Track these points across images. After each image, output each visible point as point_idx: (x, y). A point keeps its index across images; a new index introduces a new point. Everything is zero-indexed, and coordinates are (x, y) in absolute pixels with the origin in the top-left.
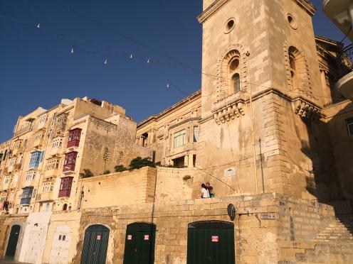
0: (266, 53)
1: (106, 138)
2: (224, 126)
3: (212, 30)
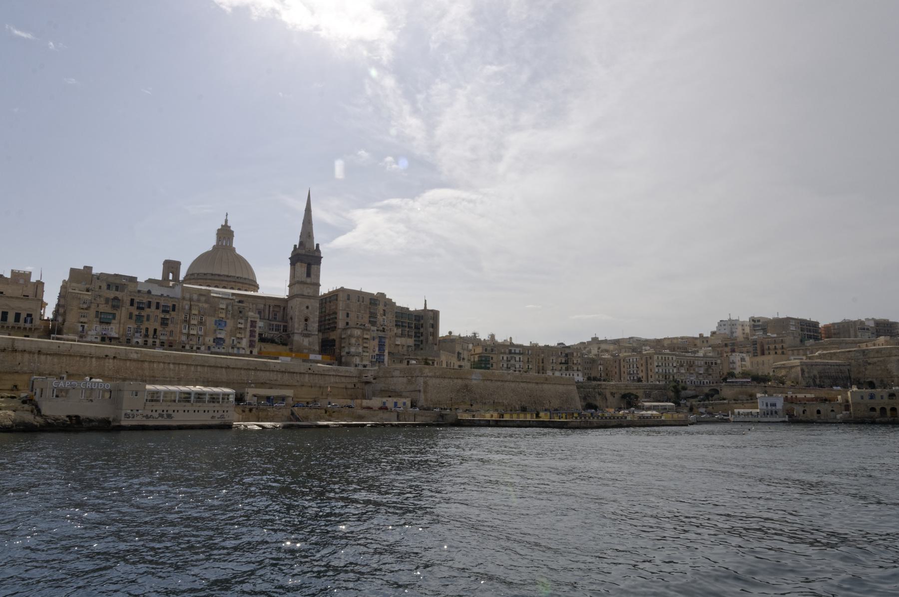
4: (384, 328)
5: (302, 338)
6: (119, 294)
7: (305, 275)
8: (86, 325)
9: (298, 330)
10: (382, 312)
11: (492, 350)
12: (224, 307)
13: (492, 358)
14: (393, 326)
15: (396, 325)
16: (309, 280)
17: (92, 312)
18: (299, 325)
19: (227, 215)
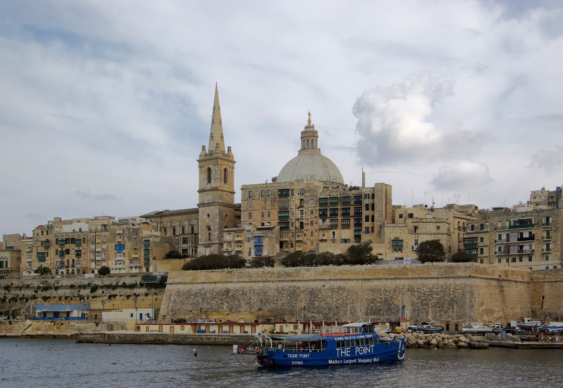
0: (217, 232)
1: (158, 242)
2: (206, 248)
3: (202, 212)
4: (302, 224)
5: (205, 249)
6: (49, 237)
7: (206, 182)
8: (32, 264)
9: (202, 241)
10: (298, 203)
11: (482, 226)
12: (121, 232)
13: (482, 239)
14: (316, 217)
15: (320, 215)
16: (209, 187)
17: (34, 254)
18: (202, 236)
19: (309, 115)
